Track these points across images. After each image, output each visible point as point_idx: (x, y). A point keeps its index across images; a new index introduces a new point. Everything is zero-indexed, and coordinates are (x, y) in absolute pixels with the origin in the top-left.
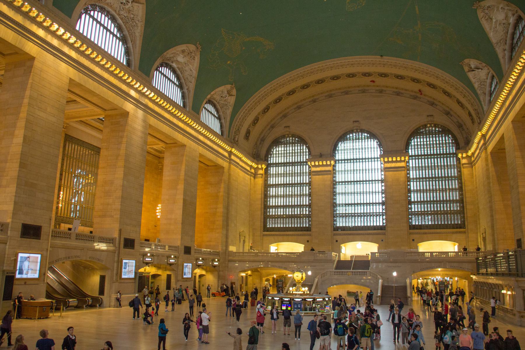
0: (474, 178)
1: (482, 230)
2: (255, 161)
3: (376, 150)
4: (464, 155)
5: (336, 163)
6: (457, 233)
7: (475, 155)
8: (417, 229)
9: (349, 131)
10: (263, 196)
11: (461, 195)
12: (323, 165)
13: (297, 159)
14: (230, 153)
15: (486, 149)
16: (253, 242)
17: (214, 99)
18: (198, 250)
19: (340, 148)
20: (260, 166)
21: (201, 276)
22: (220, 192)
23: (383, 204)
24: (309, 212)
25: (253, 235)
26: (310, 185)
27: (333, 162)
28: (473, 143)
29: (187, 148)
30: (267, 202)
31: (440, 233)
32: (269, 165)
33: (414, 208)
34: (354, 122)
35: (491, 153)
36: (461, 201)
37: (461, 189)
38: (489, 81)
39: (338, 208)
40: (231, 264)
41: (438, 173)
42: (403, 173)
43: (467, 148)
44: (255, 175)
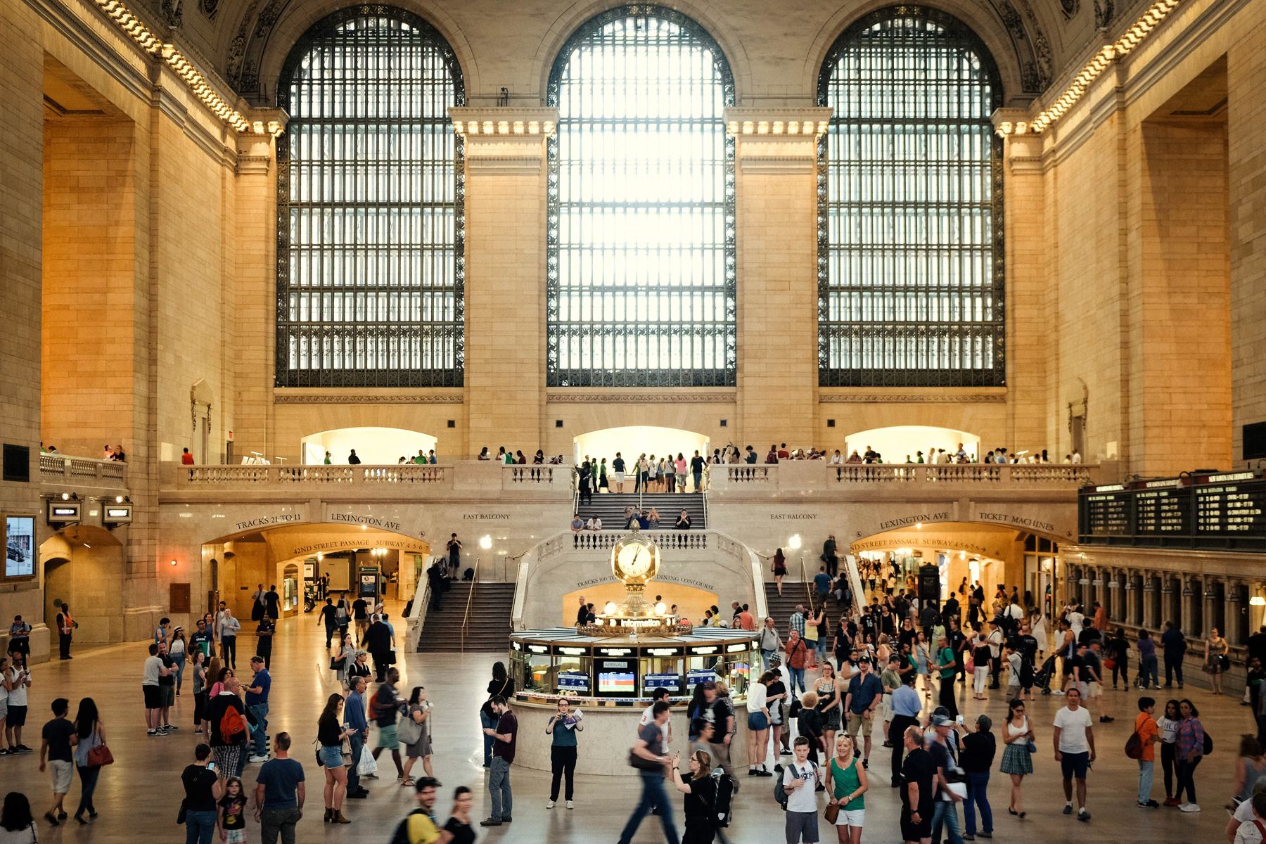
0: (1050, 212)
1: (1069, 391)
2: (242, 103)
3: (708, 88)
4: (1021, 129)
5: (558, 130)
6: (976, 399)
7: (1063, 132)
8: (843, 385)
9: (613, 10)
10: (272, 247)
11: (999, 268)
13: (406, 106)
15: (1122, 109)
16: (238, 426)
18: (51, 461)
19: (575, 75)
21: (53, 564)
22: (117, 223)
23: (730, 290)
24: (458, 312)
25: (238, 400)
26: (459, 213)
28: (1068, 82)
30: (288, 273)
31: (921, 400)
32: (295, 124)
33: (841, 309)
35: (1147, 124)
36: (998, 290)
37: (998, 248)
39: (564, 300)
40: (166, 514)
41: (910, 186)
42: (806, 183)
43: (1036, 103)
44: (239, 162)
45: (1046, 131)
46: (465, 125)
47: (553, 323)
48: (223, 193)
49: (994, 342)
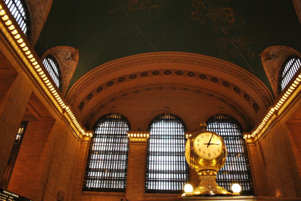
2: (84, 128)
3: (181, 129)
7: (259, 136)
9: (162, 115)
12: (140, 137)
14: (64, 110)
17: (59, 59)
19: (154, 127)
20: (87, 134)
24: (125, 175)
27: (148, 135)
29: (18, 77)
30: (89, 166)
32: (95, 136)
34: (166, 107)
35: (287, 123)
36: (249, 172)
38: (279, 69)
39: (150, 174)
43: (252, 130)
45: (255, 136)
46: (130, 135)
47: (147, 178)
48: (77, 147)
49: (249, 184)
